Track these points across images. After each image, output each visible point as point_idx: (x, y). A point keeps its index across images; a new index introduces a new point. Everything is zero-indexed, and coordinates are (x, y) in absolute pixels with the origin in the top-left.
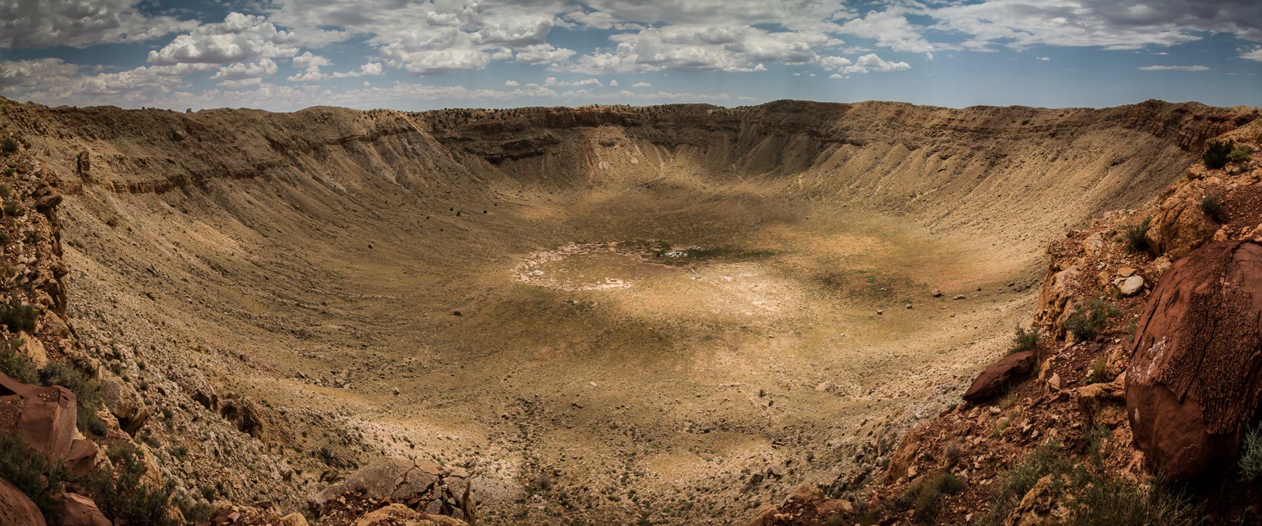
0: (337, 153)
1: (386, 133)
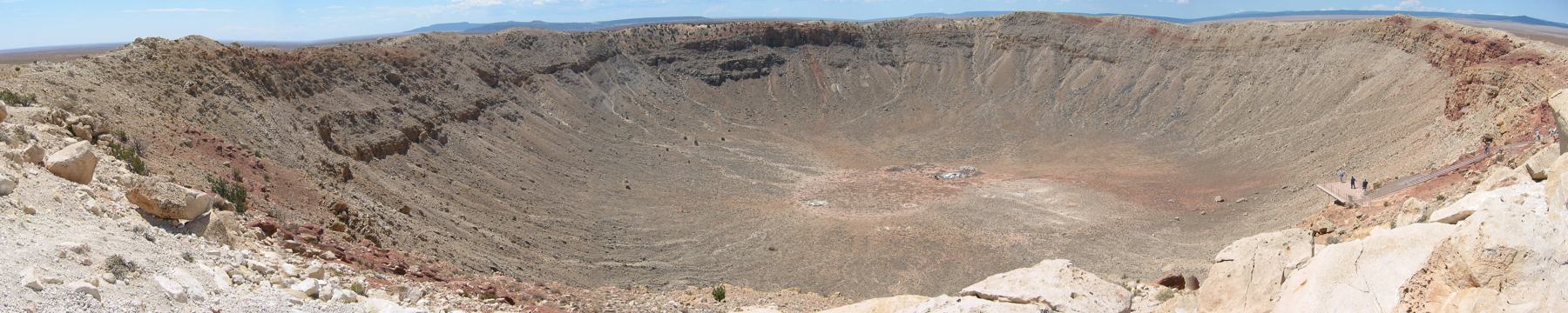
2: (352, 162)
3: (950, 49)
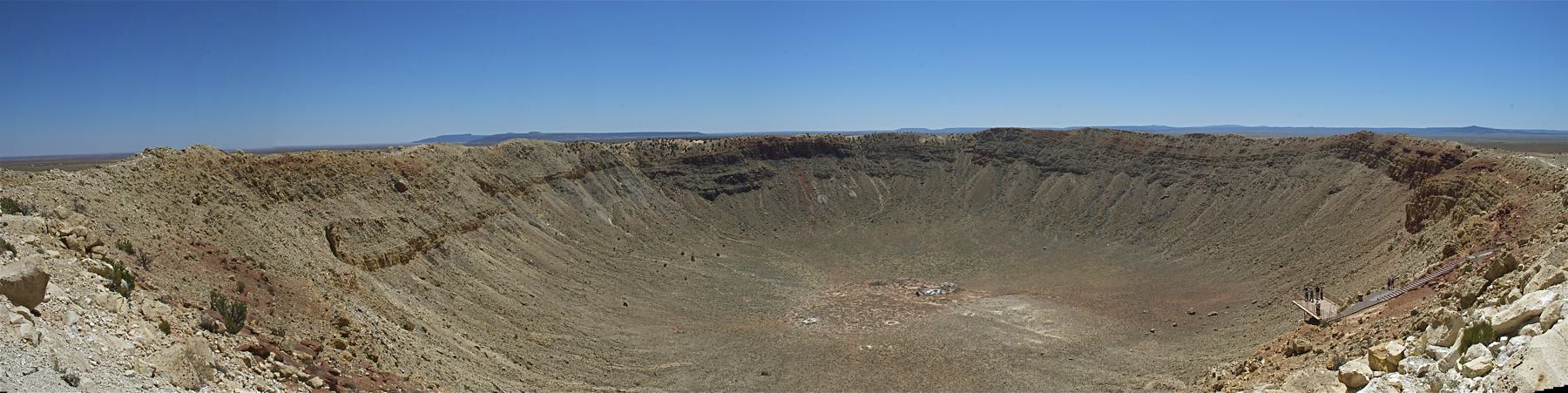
0: (546, 193)
1: (593, 169)
2: (359, 272)
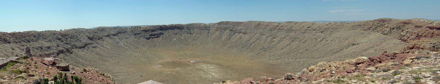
3: (204, 31)
